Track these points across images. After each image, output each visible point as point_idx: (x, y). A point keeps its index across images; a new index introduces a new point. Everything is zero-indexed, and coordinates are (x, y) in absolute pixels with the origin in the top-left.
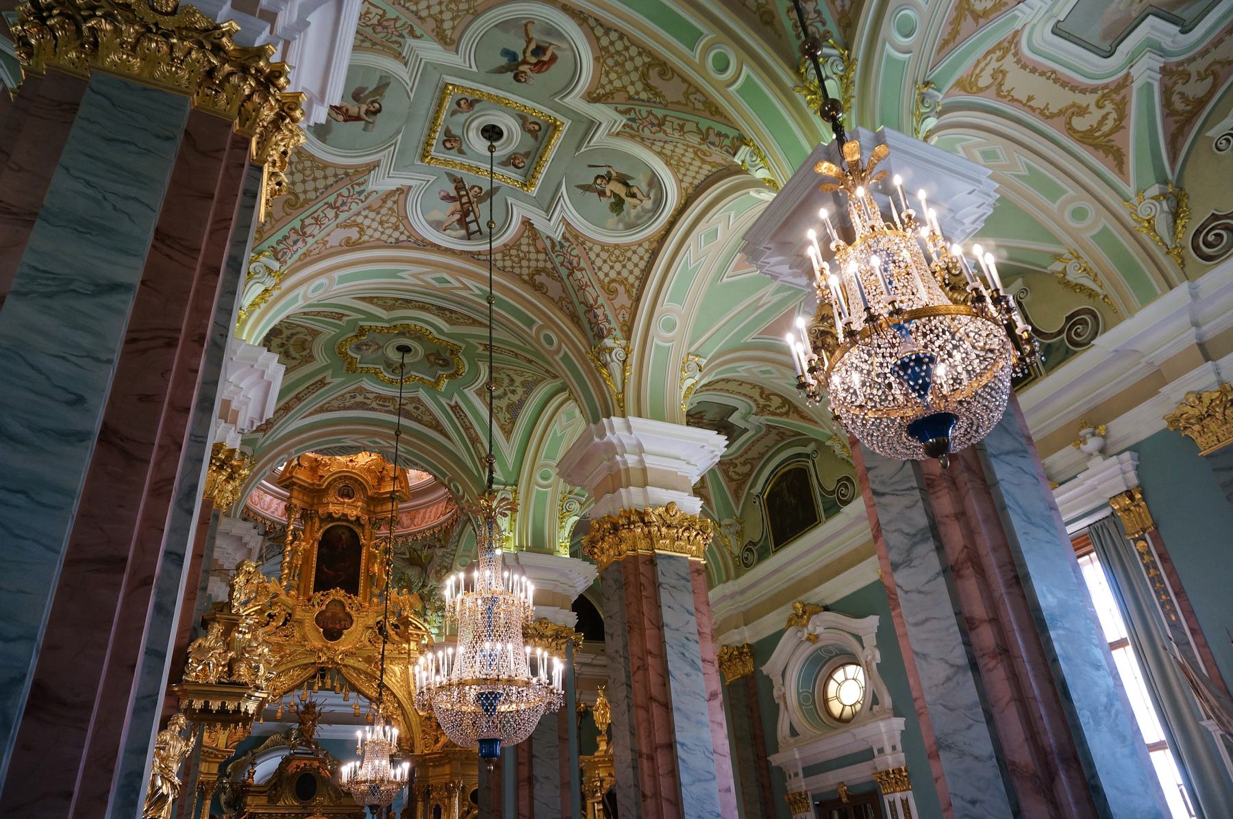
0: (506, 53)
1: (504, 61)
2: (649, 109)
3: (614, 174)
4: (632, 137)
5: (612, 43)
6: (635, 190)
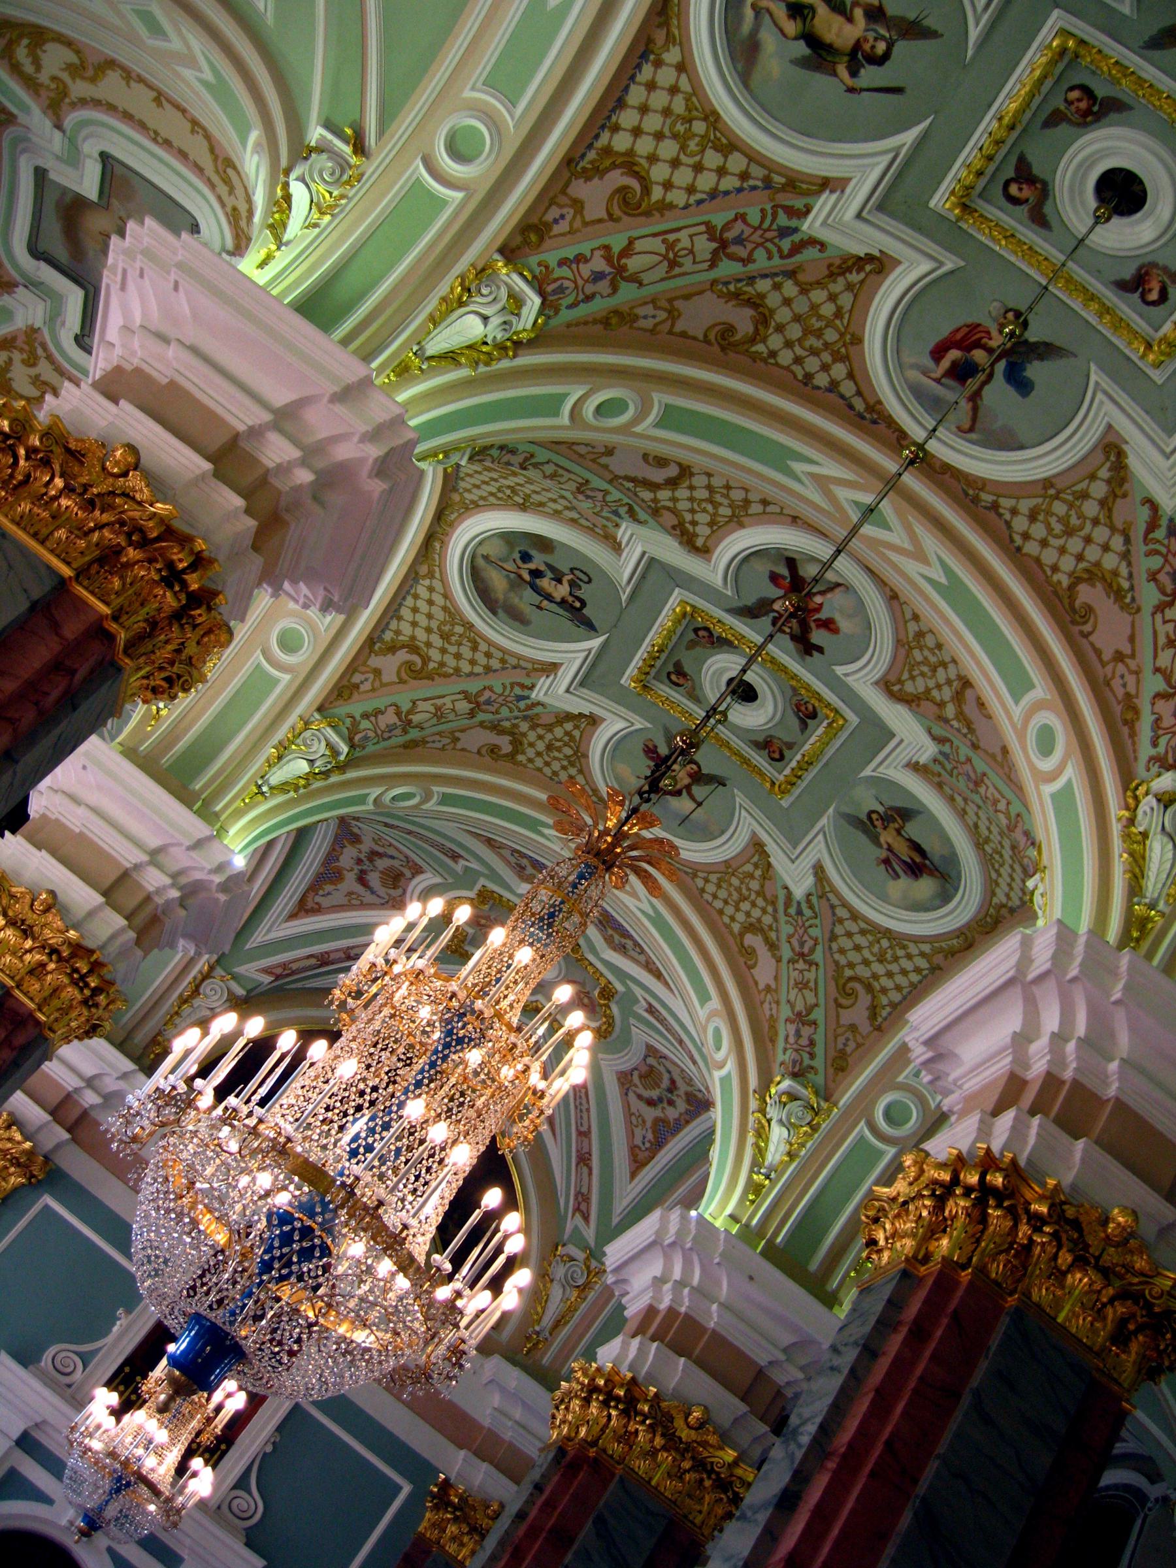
0: (1023, 386)
1: (1035, 370)
2: (751, 267)
3: (842, 70)
4: (793, 182)
5: (825, 368)
6: (791, 27)
